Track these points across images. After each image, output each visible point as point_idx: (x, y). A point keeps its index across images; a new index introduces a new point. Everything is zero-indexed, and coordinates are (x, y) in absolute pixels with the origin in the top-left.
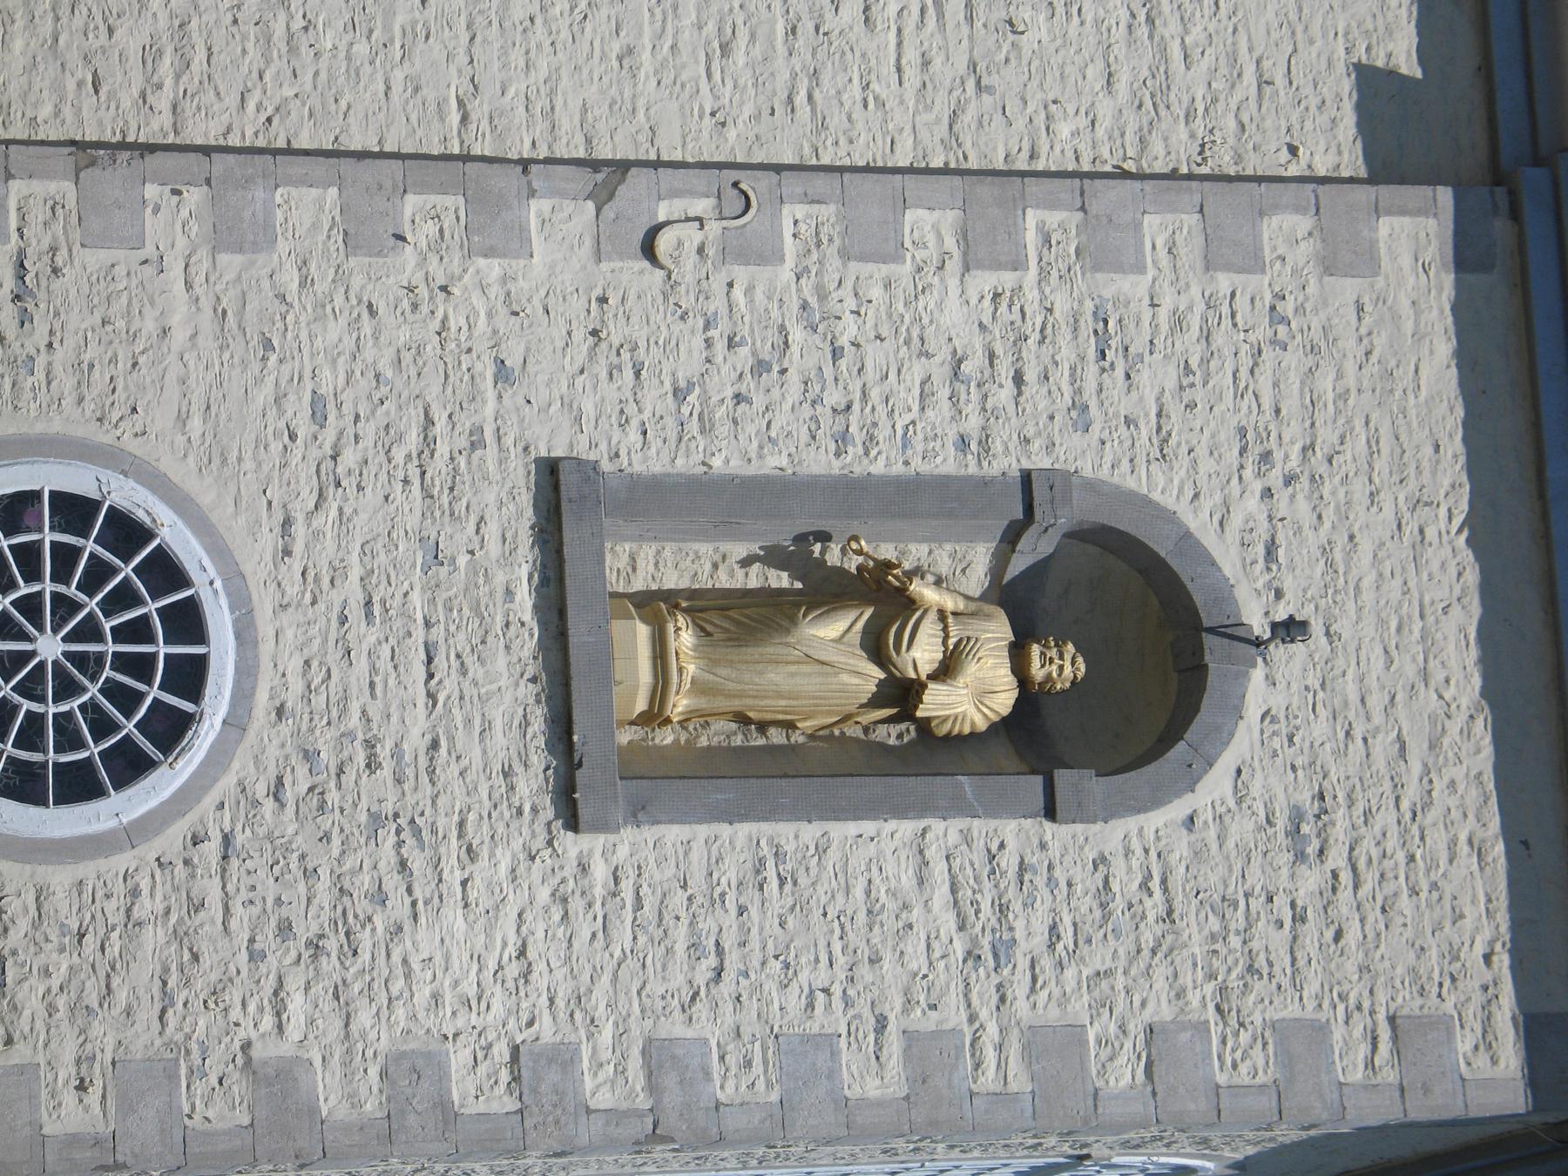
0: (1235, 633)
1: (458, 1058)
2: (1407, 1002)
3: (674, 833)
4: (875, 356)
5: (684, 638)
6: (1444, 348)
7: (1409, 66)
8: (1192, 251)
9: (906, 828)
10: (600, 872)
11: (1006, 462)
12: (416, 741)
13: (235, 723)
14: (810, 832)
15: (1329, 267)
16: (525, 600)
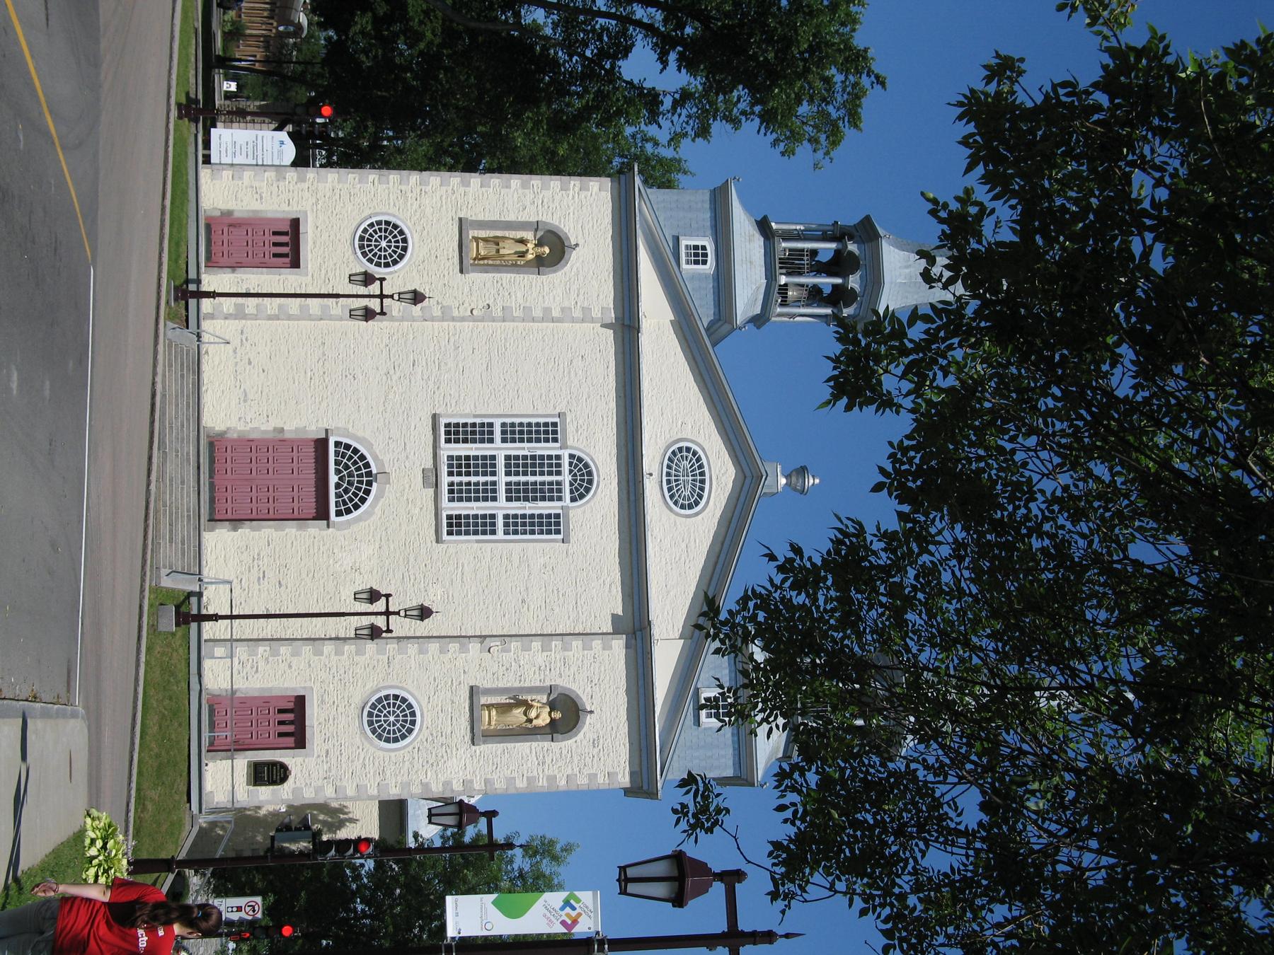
0: (585, 711)
1: (454, 782)
2: (611, 770)
3: (490, 746)
4: (526, 667)
5: (494, 712)
6: (623, 662)
7: (620, 613)
8: (580, 647)
9: (529, 744)
10: (478, 752)
11: (548, 684)
12: (449, 732)
13: (420, 730)
14: (513, 745)
15: (604, 649)
16: (467, 709)
